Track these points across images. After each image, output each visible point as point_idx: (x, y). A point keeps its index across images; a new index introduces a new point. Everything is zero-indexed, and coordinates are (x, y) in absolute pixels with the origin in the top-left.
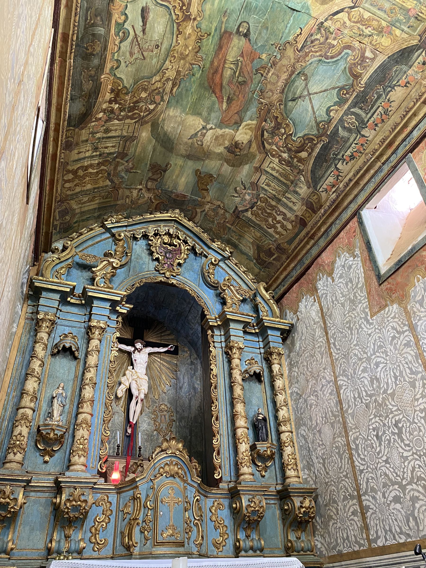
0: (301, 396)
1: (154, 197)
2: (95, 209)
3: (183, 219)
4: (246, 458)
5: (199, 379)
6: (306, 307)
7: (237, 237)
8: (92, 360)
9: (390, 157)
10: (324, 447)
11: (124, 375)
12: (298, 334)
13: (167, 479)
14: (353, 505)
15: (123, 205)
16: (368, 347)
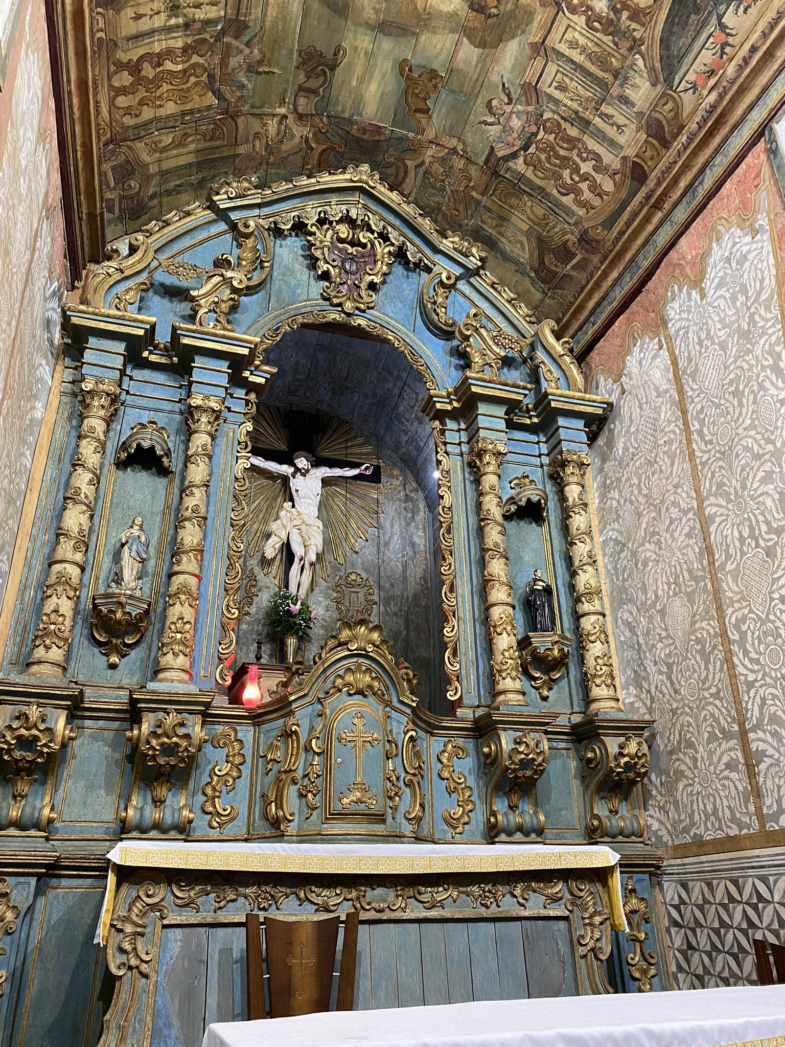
0: (624, 545)
1: (315, 135)
2: (190, 165)
3: (379, 187)
4: (510, 661)
5: (421, 527)
6: (641, 363)
7: (495, 222)
8: (197, 473)
10: (671, 641)
11: (277, 518)
12: (621, 423)
13: (350, 698)
14: (731, 750)
15: (249, 157)
16: (776, 428)
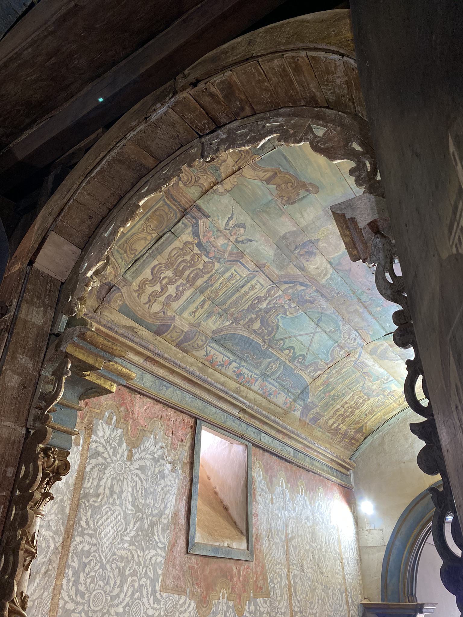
9: (243, 421)
